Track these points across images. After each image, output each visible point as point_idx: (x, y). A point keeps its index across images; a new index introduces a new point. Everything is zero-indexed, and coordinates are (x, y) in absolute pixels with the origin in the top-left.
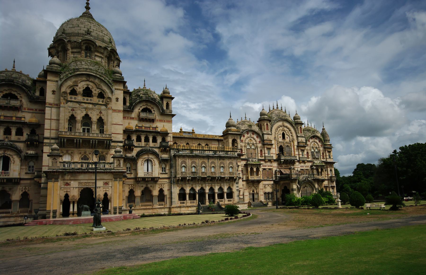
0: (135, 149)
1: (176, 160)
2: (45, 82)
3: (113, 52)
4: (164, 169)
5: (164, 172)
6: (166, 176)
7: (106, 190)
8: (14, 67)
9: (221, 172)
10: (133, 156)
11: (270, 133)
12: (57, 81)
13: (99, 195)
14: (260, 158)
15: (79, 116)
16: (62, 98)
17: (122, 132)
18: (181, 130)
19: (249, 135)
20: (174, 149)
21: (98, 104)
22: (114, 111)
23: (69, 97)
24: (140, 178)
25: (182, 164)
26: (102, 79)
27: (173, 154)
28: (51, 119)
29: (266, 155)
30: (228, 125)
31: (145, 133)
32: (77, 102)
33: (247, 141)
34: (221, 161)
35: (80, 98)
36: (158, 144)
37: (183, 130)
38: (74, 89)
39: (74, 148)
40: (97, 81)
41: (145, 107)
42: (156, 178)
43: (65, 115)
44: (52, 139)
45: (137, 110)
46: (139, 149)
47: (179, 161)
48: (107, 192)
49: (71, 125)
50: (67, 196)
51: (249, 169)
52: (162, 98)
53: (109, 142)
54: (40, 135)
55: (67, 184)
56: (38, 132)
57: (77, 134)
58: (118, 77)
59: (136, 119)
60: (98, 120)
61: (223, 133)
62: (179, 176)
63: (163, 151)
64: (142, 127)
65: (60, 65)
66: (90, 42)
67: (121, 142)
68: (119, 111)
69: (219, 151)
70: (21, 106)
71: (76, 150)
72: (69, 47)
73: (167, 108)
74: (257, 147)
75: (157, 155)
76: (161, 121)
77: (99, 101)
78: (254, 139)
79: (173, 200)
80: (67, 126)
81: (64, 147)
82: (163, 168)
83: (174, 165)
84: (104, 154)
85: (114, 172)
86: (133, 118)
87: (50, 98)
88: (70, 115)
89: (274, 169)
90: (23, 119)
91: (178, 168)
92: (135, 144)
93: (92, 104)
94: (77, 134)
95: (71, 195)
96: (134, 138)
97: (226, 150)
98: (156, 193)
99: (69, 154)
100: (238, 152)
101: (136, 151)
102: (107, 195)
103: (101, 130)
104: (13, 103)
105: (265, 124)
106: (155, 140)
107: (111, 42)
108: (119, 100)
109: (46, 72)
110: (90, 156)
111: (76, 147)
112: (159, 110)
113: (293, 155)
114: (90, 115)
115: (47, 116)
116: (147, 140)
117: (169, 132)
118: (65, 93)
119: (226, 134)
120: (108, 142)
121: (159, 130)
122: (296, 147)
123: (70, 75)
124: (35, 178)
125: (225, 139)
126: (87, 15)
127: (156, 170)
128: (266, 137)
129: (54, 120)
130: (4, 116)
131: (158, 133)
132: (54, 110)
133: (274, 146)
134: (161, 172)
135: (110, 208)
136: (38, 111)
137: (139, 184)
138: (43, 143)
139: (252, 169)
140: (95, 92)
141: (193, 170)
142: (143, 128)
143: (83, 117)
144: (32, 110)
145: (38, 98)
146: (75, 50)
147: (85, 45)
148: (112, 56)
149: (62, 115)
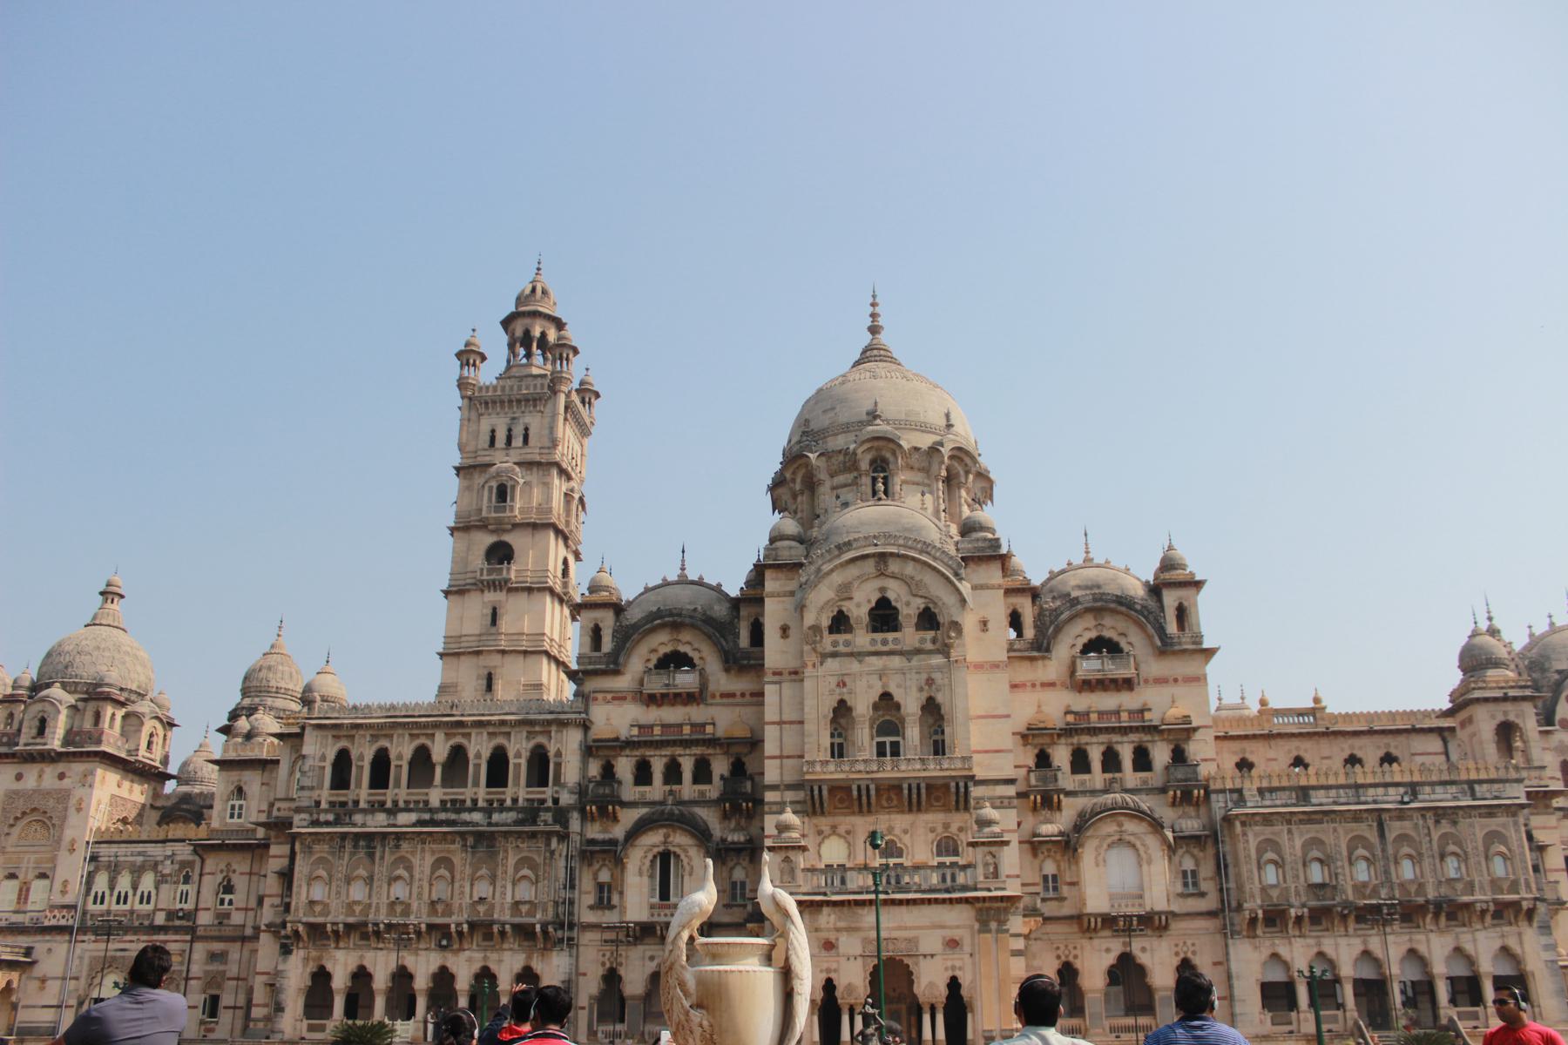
0: (1065, 801)
1: (1233, 836)
2: (760, 601)
3: (962, 455)
4: (1189, 879)
5: (1191, 890)
7: (953, 968)
8: (683, 569)
9: (1450, 881)
10: (1061, 834)
12: (792, 594)
13: (931, 985)
15: (863, 705)
16: (807, 648)
17: (1008, 742)
18: (1263, 703)
20: (1223, 791)
21: (918, 651)
23: (828, 640)
24: (1096, 916)
25: (1260, 851)
26: (925, 563)
27: (1219, 815)
28: (781, 723)
30: (1474, 661)
31: (1103, 738)
32: (851, 655)
34: (1446, 827)
35: (862, 638)
36: (1155, 777)
37: (1274, 704)
38: (840, 612)
39: (853, 813)
40: (910, 569)
41: (1093, 634)
42: (1160, 913)
43: (818, 707)
44: (789, 787)
47: (1251, 840)
48: (958, 973)
49: (840, 735)
50: (829, 986)
52: (1155, 590)
53: (966, 787)
54: (757, 778)
57: (861, 767)
58: (980, 544)
59: (1063, 685)
60: (923, 708)
61: (1453, 696)
62: (1254, 904)
63: (1181, 804)
64: (1088, 714)
65: (800, 540)
66: (881, 443)
68: (995, 666)
69: (1432, 784)
70: (704, 685)
72: (823, 476)
75: (1157, 826)
76: (1161, 681)
77: (923, 641)
79: (1238, 1010)
80: (826, 741)
81: (823, 813)
82: (1185, 873)
83: (1229, 859)
84: (954, 828)
85: (977, 899)
86: (1052, 685)
87: (775, 652)
90: (709, 729)
91: (1248, 869)
92: (1067, 780)
93: (901, 653)
95: (841, 982)
96: (1061, 756)
97: (1464, 777)
98: (1163, 977)
99: (840, 836)
100: (1535, 782)
101: (1070, 809)
102: (959, 986)
103: (936, 742)
104: (685, 680)
106: (1142, 760)
108: (989, 625)
109: (759, 571)
110: (906, 839)
111: (861, 812)
112: (1150, 637)
114: (898, 695)
115: (770, 713)
116: (1111, 761)
118: (816, 629)
119: (1461, 703)
120: (962, 784)
121: (1153, 717)
123: (826, 568)
124: (748, 921)
125: (1463, 725)
126: (872, 354)
127: (1157, 883)
129: (791, 723)
130: (663, 726)
131: (1153, 729)
132: (788, 689)
134: (1179, 888)
135: (970, 1036)
136: (748, 699)
137: (1096, 942)
140: (909, 610)
141: (1317, 874)
142: (1094, 717)
143: (876, 707)
144: (733, 695)
145: (747, 655)
146: (841, 479)
147: (869, 457)
148: (958, 471)
149: (809, 703)
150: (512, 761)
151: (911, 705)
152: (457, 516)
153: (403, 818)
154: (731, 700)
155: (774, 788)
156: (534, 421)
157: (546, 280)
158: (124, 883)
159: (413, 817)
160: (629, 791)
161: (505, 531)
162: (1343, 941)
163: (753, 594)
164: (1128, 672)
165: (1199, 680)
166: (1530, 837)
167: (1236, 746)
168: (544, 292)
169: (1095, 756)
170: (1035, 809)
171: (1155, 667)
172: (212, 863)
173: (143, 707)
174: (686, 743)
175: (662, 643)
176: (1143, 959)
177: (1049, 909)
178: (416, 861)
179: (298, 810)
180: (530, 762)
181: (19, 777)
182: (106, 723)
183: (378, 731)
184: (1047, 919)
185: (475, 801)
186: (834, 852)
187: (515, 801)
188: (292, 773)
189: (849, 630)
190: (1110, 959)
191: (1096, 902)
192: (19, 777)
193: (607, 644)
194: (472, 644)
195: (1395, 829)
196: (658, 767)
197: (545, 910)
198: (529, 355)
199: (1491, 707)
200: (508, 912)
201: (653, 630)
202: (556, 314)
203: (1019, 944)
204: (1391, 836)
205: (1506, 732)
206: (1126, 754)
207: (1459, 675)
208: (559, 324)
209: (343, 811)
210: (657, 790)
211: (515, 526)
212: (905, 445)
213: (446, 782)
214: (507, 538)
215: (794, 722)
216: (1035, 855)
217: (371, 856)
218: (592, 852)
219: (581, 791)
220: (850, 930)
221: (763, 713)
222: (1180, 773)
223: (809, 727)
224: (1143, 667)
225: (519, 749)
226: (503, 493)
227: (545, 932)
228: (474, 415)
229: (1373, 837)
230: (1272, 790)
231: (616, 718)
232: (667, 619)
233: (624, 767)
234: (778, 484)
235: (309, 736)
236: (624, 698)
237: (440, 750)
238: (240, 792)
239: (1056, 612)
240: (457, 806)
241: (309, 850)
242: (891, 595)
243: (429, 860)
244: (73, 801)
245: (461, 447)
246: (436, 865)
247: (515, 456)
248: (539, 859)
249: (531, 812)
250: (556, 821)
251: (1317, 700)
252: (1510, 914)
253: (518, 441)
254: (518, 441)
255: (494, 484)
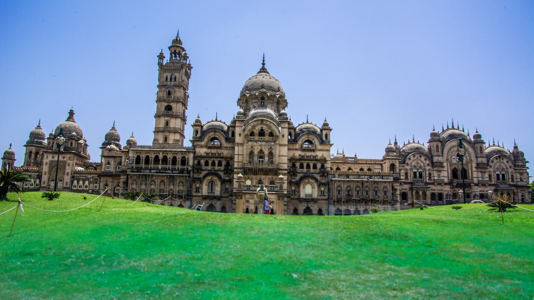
3: (282, 96)
4: (322, 193)
6: (324, 198)
11: (441, 154)
14: (428, 181)
15: (256, 152)
17: (286, 161)
19: (416, 158)
20: (331, 174)
21: (269, 141)
22: (281, 145)
25: (337, 187)
28: (238, 155)
29: (436, 178)
30: (389, 150)
31: (307, 162)
33: (413, 164)
34: (376, 185)
35: (257, 138)
36: (318, 171)
41: (307, 139)
45: (300, 142)
46: (301, 175)
51: (414, 193)
55: (248, 201)
56: (231, 163)
59: (300, 150)
62: (335, 198)
67: (286, 170)
68: (285, 145)
71: (254, 176)
73: (326, 139)
74: (425, 170)
75: (316, 180)
76: (320, 150)
78: (422, 161)
80: (248, 159)
86: (296, 149)
88: (249, 151)
89: (445, 193)
92: (299, 170)
93: (265, 141)
94: (255, 165)
96: (298, 165)
105: (435, 146)
106: (315, 167)
107: (279, 91)
112: (319, 141)
113: (470, 178)
115: (236, 153)
116: (308, 166)
117: (327, 159)
118: (246, 135)
119: (384, 159)
121: (318, 158)
122: (474, 169)
126: (263, 70)
128: (435, 159)
131: (318, 160)
132: (240, 148)
133: (446, 169)
134: (320, 194)
138: (233, 171)
139: (417, 193)
140: (267, 131)
143: (259, 152)
144: (227, 147)
146: (254, 101)
151: (266, 152)
152: (158, 97)
153: (153, 171)
155: (236, 168)
156: (177, 75)
157: (181, 37)
158: (81, 183)
159: (155, 171)
160: (204, 168)
161: (170, 103)
162: (352, 207)
163: (233, 125)
164: (314, 148)
165: (328, 150)
166: (393, 187)
167: (337, 164)
168: (180, 40)
169: (305, 165)
170: (291, 176)
171: (319, 147)
172: (102, 179)
173: (81, 141)
174: (217, 158)
175: (212, 135)
176: (312, 208)
177: (292, 197)
178: (156, 181)
179: (128, 168)
180: (182, 160)
181: (53, 157)
182: (73, 145)
183: (146, 152)
184: (292, 199)
185: (169, 168)
186: (248, 182)
187: (178, 168)
188: (125, 160)
189: (254, 135)
190: (304, 208)
191: (302, 195)
192: (53, 157)
193: (199, 135)
194: (162, 129)
195: (365, 184)
196: (210, 162)
198: (175, 57)
199: (390, 160)
201: (210, 132)
202: (183, 46)
203: (286, 203)
204: (364, 186)
205: (392, 167)
206: (312, 165)
207: (385, 153)
208: (184, 50)
209: (139, 170)
210: (210, 167)
211: (172, 101)
212: (269, 94)
213: (162, 164)
214: (171, 104)
215: (240, 154)
216: (290, 185)
217: (146, 179)
218: (195, 180)
219: (193, 167)
220: (252, 198)
221: (234, 152)
222: (322, 170)
223: (245, 156)
224: (317, 147)
225: (179, 157)
226: (169, 93)
227: (185, 197)
228: (162, 72)
229: (361, 186)
230: (341, 175)
231: (202, 151)
232: (214, 129)
233: (203, 162)
234: (239, 100)
235: (130, 152)
237: (161, 156)
238: (109, 163)
239: (299, 134)
240: (166, 169)
241: (131, 177)
242: (264, 129)
243: (159, 181)
244: (67, 164)
245: (159, 80)
246: (161, 182)
247: (172, 83)
248: (184, 182)
249: (182, 171)
250: (187, 173)
251: (356, 156)
252: (386, 203)
253: (173, 80)
254: (173, 80)
255: (167, 90)
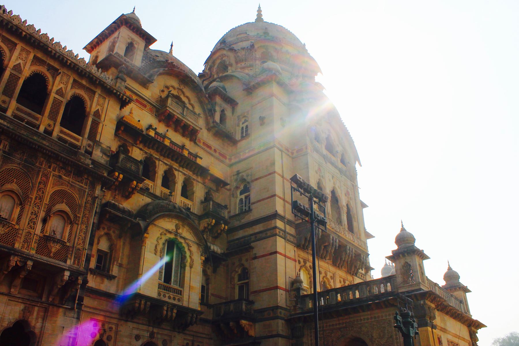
144: (209, 147)
150: (53, 95)
154: (208, 150)
197: (78, 258)
200: (34, 245)
236: (145, 106)
